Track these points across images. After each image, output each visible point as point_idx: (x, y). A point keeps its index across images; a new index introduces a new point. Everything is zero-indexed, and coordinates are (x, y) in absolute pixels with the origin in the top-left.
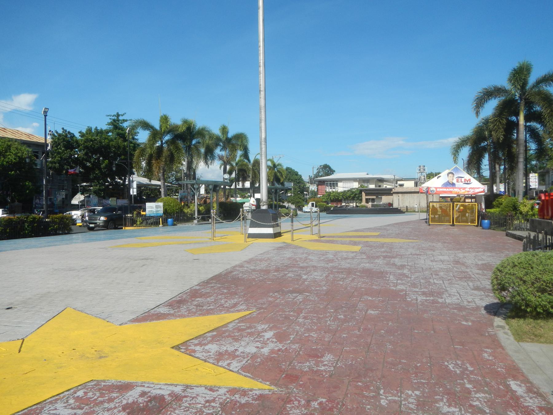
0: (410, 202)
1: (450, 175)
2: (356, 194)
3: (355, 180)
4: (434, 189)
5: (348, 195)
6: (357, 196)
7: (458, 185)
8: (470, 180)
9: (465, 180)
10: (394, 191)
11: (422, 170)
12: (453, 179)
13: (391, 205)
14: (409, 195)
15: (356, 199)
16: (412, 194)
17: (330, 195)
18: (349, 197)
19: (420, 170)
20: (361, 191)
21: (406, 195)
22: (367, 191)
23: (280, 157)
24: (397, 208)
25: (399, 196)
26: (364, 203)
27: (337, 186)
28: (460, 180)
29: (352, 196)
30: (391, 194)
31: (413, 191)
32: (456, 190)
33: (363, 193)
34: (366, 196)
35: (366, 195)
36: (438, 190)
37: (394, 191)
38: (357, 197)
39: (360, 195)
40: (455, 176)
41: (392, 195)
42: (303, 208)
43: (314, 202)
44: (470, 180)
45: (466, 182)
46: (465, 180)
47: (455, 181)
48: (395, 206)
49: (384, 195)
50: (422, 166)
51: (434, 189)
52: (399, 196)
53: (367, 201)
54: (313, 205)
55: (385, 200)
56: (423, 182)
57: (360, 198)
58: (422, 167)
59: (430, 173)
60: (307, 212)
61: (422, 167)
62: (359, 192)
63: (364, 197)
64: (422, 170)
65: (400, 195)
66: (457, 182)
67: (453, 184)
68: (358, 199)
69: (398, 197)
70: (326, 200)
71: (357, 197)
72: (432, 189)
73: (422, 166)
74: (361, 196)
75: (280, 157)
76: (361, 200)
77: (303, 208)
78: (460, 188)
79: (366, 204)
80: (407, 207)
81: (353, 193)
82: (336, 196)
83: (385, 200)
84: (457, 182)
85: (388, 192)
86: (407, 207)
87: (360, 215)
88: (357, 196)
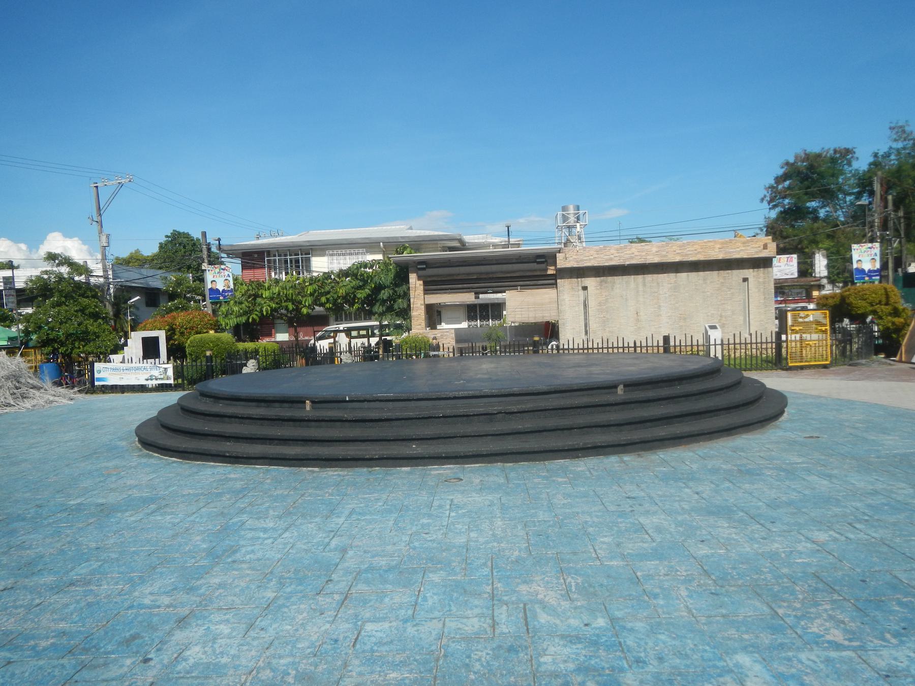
2: (379, 288)
3: (370, 245)
5: (342, 292)
10: (562, 262)
11: (572, 219)
13: (550, 330)
16: (649, 278)
17: (256, 296)
18: (350, 299)
21: (619, 281)
22: (430, 272)
23: (121, 185)
26: (418, 327)
27: (308, 269)
29: (361, 294)
30: (550, 281)
31: (656, 260)
33: (413, 278)
34: (426, 291)
35: (431, 286)
37: (562, 262)
38: (384, 302)
39: (400, 290)
41: (555, 285)
42: (97, 366)
43: (162, 335)
49: (514, 287)
50: (571, 207)
54: (150, 349)
57: (400, 303)
58: (572, 210)
60: (114, 389)
61: (572, 210)
64: (572, 219)
65: (591, 282)
68: (390, 309)
69: (581, 292)
70: (243, 319)
73: (571, 207)
74: (406, 295)
75: (121, 185)
76: (405, 313)
77: (97, 366)
79: (430, 334)
80: (666, 339)
81: (365, 280)
82: (287, 300)
86: (666, 339)
88: (384, 294)
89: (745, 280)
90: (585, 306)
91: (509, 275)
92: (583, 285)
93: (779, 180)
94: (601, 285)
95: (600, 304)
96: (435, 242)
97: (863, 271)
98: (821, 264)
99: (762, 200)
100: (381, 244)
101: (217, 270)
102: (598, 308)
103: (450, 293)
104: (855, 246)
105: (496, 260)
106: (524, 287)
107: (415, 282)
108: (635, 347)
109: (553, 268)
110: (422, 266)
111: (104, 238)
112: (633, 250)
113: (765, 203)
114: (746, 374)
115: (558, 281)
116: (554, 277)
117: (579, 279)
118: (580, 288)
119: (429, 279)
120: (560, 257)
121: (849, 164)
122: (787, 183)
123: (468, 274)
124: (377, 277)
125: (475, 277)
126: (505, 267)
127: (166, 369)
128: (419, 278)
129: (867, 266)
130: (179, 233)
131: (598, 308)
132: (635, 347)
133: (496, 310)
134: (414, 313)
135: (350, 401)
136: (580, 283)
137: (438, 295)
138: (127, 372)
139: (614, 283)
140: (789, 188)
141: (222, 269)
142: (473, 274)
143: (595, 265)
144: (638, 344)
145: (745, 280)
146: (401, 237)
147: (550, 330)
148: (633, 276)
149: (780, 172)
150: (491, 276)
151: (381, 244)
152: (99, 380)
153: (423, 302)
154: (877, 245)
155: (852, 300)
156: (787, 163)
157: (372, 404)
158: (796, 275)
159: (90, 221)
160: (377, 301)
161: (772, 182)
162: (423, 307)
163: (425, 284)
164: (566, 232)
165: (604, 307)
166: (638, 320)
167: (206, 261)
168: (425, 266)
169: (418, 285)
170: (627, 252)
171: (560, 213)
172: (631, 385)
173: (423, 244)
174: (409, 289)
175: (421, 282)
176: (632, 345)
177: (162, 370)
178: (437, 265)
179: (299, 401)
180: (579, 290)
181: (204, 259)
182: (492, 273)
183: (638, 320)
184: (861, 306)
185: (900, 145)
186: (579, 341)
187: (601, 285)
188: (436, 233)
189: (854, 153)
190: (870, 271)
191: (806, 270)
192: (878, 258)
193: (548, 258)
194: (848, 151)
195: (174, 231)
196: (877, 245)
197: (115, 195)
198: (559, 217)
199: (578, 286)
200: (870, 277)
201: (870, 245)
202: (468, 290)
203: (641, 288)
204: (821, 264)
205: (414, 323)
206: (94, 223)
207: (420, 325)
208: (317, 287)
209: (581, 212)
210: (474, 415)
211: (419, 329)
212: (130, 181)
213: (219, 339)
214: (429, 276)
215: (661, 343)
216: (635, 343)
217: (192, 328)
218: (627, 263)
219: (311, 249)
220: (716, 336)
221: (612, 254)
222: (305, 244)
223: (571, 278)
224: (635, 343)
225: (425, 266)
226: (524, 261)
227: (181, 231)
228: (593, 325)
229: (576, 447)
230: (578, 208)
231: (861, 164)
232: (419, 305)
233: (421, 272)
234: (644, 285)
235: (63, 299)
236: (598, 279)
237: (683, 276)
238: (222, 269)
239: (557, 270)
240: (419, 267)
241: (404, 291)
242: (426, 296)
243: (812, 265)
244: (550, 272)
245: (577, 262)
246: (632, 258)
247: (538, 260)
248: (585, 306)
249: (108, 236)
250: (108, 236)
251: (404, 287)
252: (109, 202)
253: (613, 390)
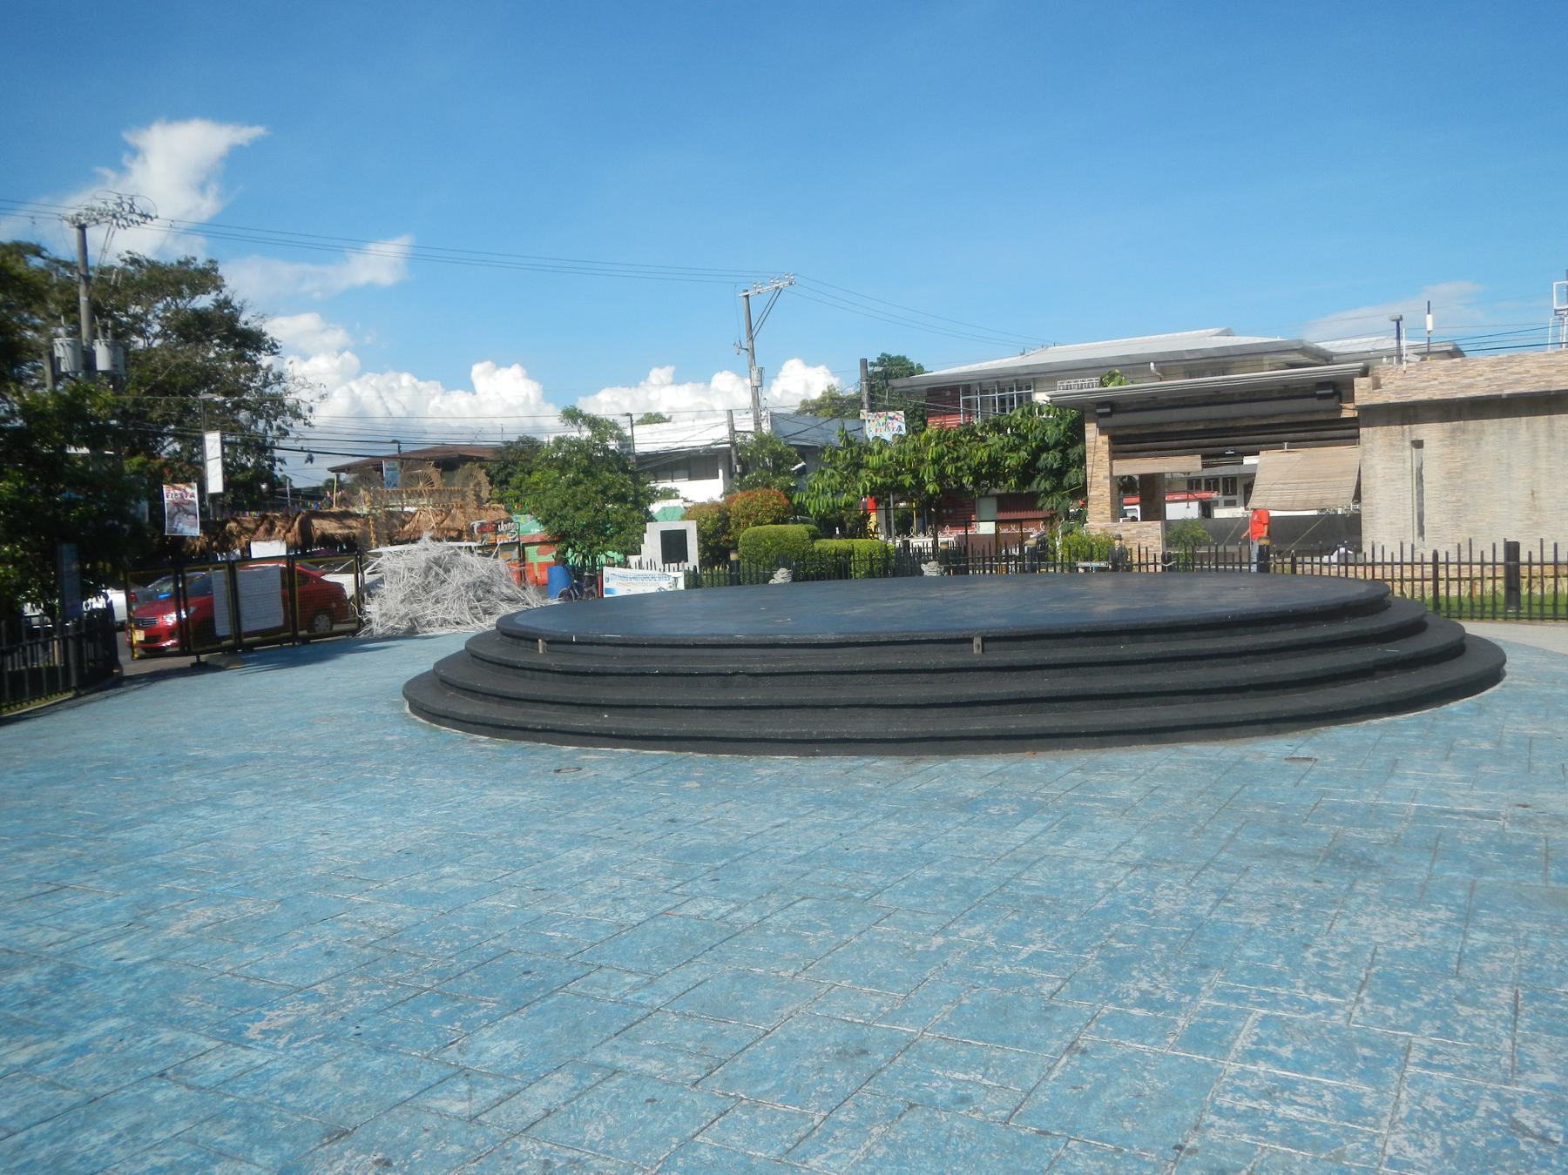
10: (1364, 393)
14: (1524, 428)
21: (1493, 429)
25: (1418, 444)
26: (1098, 521)
29: (1012, 461)
30: (1344, 431)
33: (1091, 431)
34: (1115, 454)
35: (1122, 445)
37: (1364, 393)
41: (1354, 439)
49: (1276, 444)
52: (1418, 444)
57: (1072, 477)
65: (1431, 432)
69: (1408, 452)
80: (1512, 549)
86: (1512, 549)
91: (1264, 422)
92: (1414, 438)
94: (1454, 438)
95: (1450, 474)
96: (1259, 357)
100: (1152, 365)
101: (882, 420)
102: (1445, 482)
103: (1156, 456)
105: (1241, 395)
106: (1296, 443)
107: (1095, 440)
108: (1435, 563)
109: (1350, 406)
110: (1106, 409)
111: (755, 374)
112: (1528, 365)
114: (1473, 628)
115: (1362, 430)
116: (1354, 423)
117: (1406, 427)
118: (1408, 444)
119: (1119, 433)
120: (1361, 384)
123: (1188, 422)
124: (1038, 430)
125: (1201, 427)
126: (1256, 408)
127: (676, 579)
128: (1102, 431)
130: (889, 356)
131: (1445, 482)
132: (1435, 563)
133: (1240, 487)
134: (1092, 493)
135: (577, 643)
136: (1407, 434)
137: (1135, 461)
138: (633, 581)
139: (1483, 432)
141: (892, 418)
142: (1196, 421)
143: (1435, 398)
144: (1442, 558)
146: (1188, 351)
148: (1524, 419)
150: (1230, 424)
151: (1152, 365)
152: (609, 591)
153: (1107, 474)
157: (595, 649)
159: (736, 349)
160: (1039, 471)
162: (1108, 481)
163: (1114, 440)
165: (1460, 481)
166: (1534, 508)
167: (866, 406)
168: (1108, 410)
169: (1100, 444)
170: (1517, 369)
173: (1233, 362)
175: (1106, 438)
176: (1429, 558)
177: (672, 580)
178: (1135, 407)
180: (1404, 448)
181: (863, 403)
182: (1234, 419)
183: (1534, 508)
187: (1454, 438)
188: (1258, 340)
193: (1339, 389)
195: (883, 354)
197: (770, 306)
199: (1403, 440)
202: (1188, 450)
203: (1542, 442)
205: (1091, 509)
206: (742, 352)
207: (1103, 513)
208: (945, 450)
210: (699, 675)
211: (1100, 521)
212: (791, 284)
213: (781, 534)
214: (1120, 427)
215: (1501, 558)
216: (1436, 555)
217: (748, 517)
218: (1508, 391)
219: (1034, 379)
221: (1481, 375)
222: (1021, 372)
223: (1389, 423)
224: (1436, 555)
225: (1108, 410)
226: (1296, 394)
227: (894, 354)
229: (806, 737)
232: (1101, 478)
233: (1103, 421)
234: (1551, 436)
235: (581, 475)
236: (1447, 425)
238: (892, 418)
239: (1365, 410)
240: (1099, 411)
241: (1079, 455)
242: (1115, 462)
244: (1346, 414)
245: (1397, 393)
246: (1518, 382)
247: (1319, 392)
248: (1420, 478)
249: (761, 371)
250: (761, 371)
252: (764, 318)
253: (965, 646)
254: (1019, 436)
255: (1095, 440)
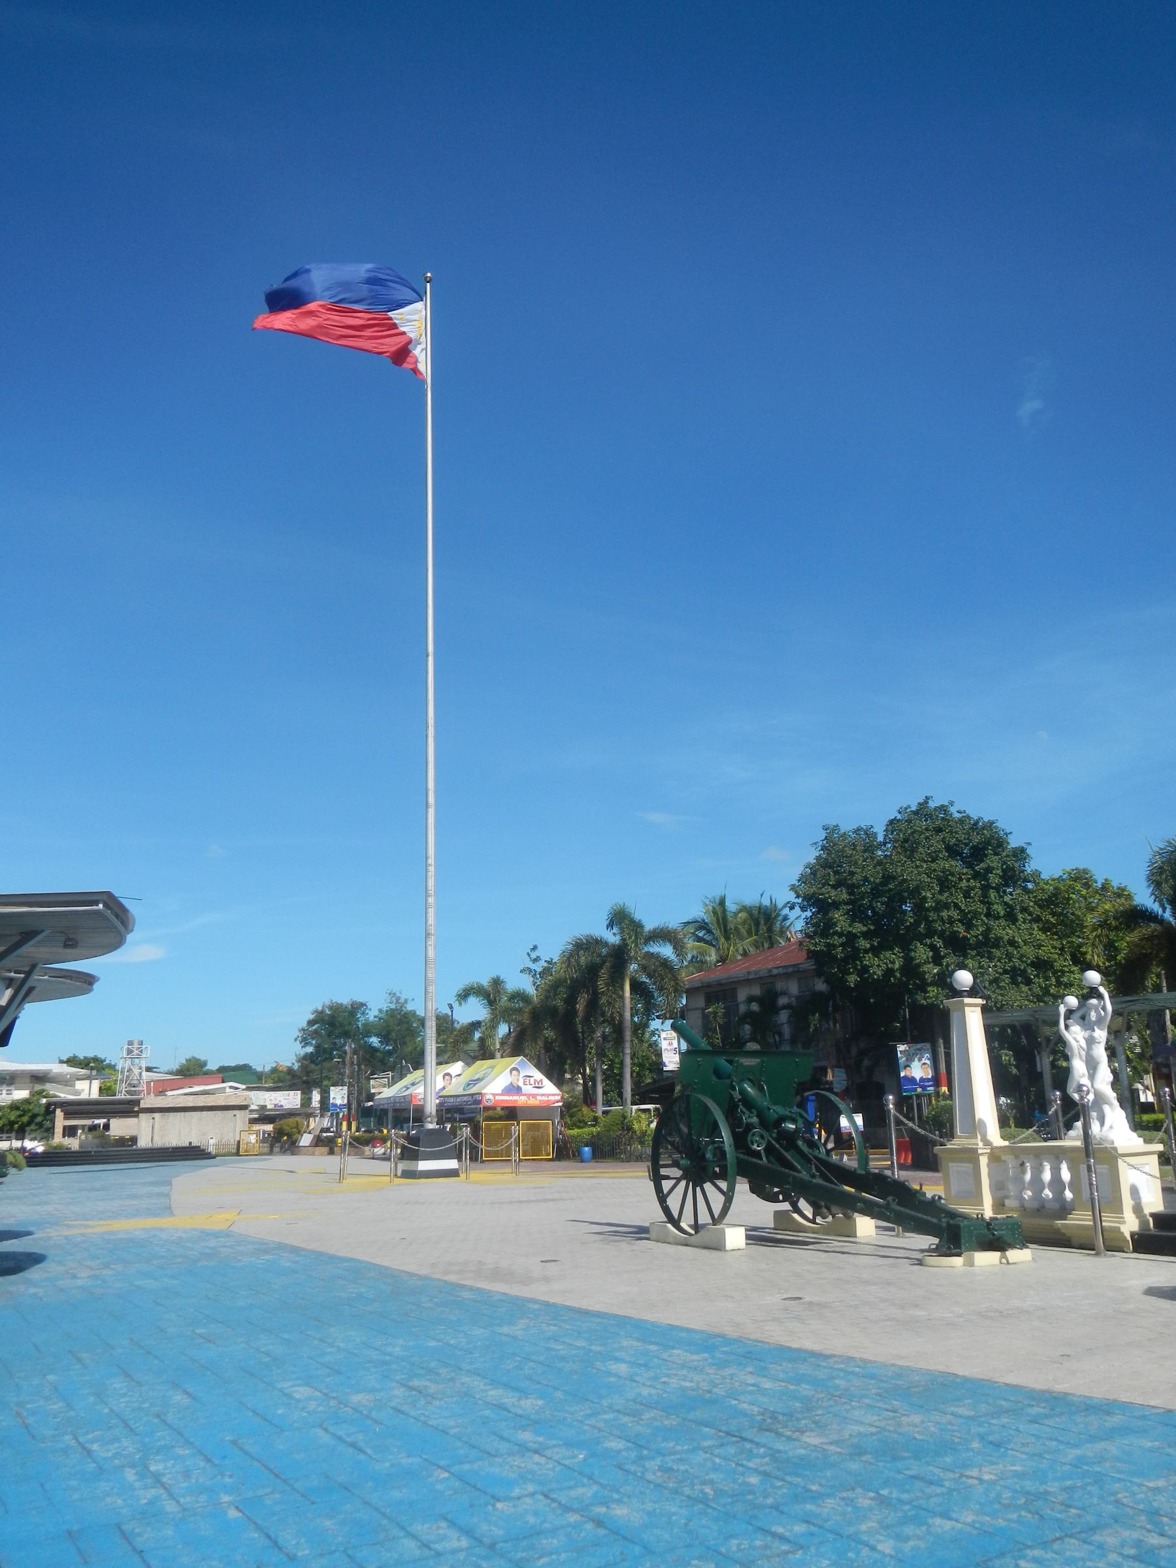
0: (180, 1132)
1: (514, 1072)
2: (35, 1116)
4: (492, 1097)
5: (12, 1118)
6: (39, 1119)
7: (528, 1089)
8: (541, 1080)
9: (535, 1081)
10: (143, 1105)
12: (518, 1080)
13: (134, 1140)
15: (33, 1127)
16: (187, 1113)
18: (12, 1123)
19: (130, 1052)
20: (49, 1110)
24: (199, 1147)
26: (58, 1139)
28: (528, 1081)
29: (25, 1119)
30: (136, 1114)
31: (191, 1105)
32: (523, 1098)
34: (65, 1118)
35: (68, 1115)
36: (497, 1098)
37: (143, 1105)
38: (37, 1124)
40: (522, 1075)
41: (137, 1116)
44: (541, 1080)
45: (537, 1085)
46: (535, 1081)
47: (521, 1084)
48: (143, 1143)
49: (115, 1117)
51: (492, 1097)
52: (153, 1118)
53: (70, 1131)
55: (119, 1127)
56: (136, 1082)
58: (136, 1046)
59: (72, 1055)
61: (136, 1046)
62: (43, 1110)
63: (60, 1121)
64: (136, 1052)
65: (157, 1116)
66: (524, 1084)
67: (518, 1090)
69: (151, 1121)
71: (37, 1124)
72: (488, 1097)
76: (50, 1131)
78: (528, 1095)
80: (190, 1143)
81: (25, 1112)
83: (119, 1127)
84: (524, 1084)
85: (129, 1109)
86: (190, 1143)
87: (182, 1162)
88: (39, 1119)
89: (235, 1115)
90: (153, 1128)
93: (311, 1023)
97: (335, 1105)
98: (316, 1097)
99: (296, 1040)
104: (332, 1088)
106: (120, 1117)
107: (59, 1114)
110: (64, 1105)
113: (298, 1042)
115: (140, 1115)
121: (363, 1013)
122: (316, 1026)
128: (62, 1111)
129: (339, 1102)
134: (56, 1131)
140: (316, 1032)
145: (235, 1115)
147: (134, 1140)
149: (312, 1017)
154: (346, 1088)
155: (284, 1126)
156: (316, 1011)
158: (299, 1106)
161: (304, 1024)
164: (129, 1062)
171: (126, 1047)
172: (173, 1148)
174: (55, 1117)
179: (91, 1152)
184: (287, 1129)
185: (393, 1006)
186: (150, 1145)
189: (366, 1005)
190: (340, 1105)
191: (307, 1101)
192: (346, 1097)
193: (137, 1102)
194: (362, 1005)
196: (346, 1088)
198: (125, 1052)
200: (341, 1109)
201: (341, 1088)
204: (316, 1097)
209: (144, 1047)
220: (212, 1142)
228: (156, 1138)
230: (141, 1043)
231: (372, 1015)
237: (205, 1113)
243: (310, 1099)
244: (136, 1109)
248: (153, 1128)
251: (53, 1115)
254: (22, 1111)
255: (59, 1114)
